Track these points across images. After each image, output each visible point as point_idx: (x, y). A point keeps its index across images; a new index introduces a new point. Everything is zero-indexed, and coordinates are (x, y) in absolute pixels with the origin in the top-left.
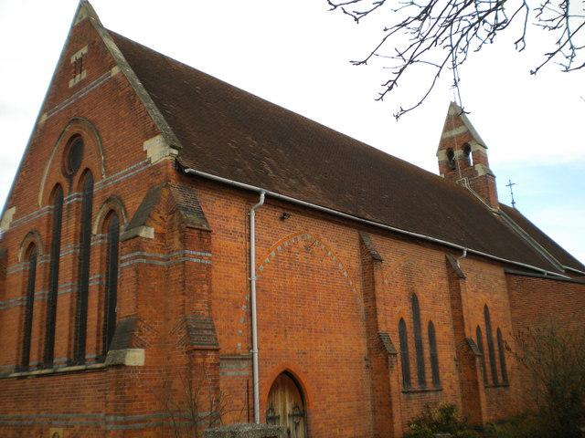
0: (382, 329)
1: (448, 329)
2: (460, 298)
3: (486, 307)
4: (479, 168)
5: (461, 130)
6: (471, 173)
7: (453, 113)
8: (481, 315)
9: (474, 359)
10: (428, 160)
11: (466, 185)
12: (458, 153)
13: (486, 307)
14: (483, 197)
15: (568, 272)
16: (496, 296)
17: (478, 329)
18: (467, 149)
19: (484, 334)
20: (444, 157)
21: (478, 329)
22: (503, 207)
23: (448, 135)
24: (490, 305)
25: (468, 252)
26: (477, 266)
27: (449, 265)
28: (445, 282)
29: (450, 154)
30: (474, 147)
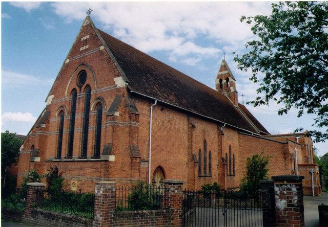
0: (194, 153)
1: (216, 154)
2: (221, 142)
3: (230, 146)
4: (231, 88)
5: (226, 72)
6: (229, 90)
7: (223, 64)
8: (228, 149)
9: (224, 165)
10: (212, 83)
11: (226, 95)
12: (224, 81)
13: (230, 146)
14: (232, 100)
15: (261, 133)
16: (234, 142)
17: (227, 154)
18: (228, 80)
19: (228, 156)
20: (218, 83)
21: (227, 154)
22: (239, 105)
23: (220, 73)
24: (232, 145)
25: (226, 125)
26: (228, 131)
27: (218, 129)
28: (217, 136)
29: (221, 81)
30: (231, 80)
